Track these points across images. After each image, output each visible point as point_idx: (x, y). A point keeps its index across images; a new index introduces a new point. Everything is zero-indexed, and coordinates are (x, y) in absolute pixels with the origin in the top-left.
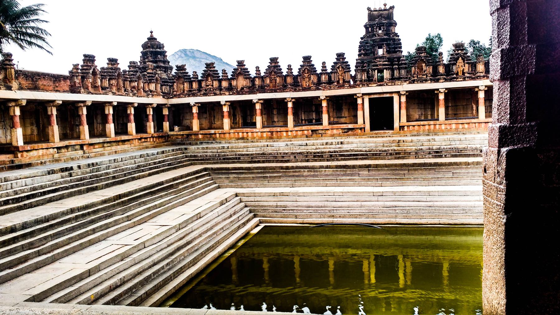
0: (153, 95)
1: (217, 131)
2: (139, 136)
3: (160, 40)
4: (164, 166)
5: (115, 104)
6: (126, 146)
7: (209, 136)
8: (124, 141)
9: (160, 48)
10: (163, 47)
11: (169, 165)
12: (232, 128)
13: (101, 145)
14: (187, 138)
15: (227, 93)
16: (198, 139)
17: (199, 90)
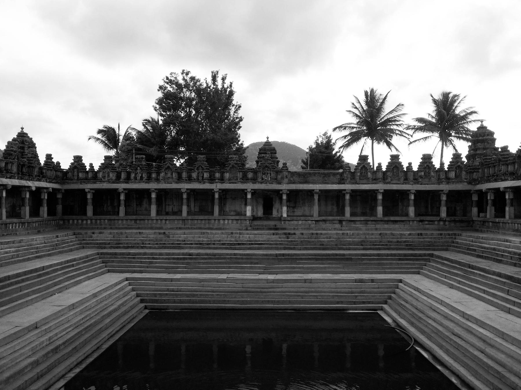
0: (448, 183)
1: (500, 219)
2: (418, 219)
3: (490, 128)
4: (397, 245)
5: (382, 191)
6: (397, 226)
7: (495, 224)
8: (396, 222)
9: (484, 136)
10: (491, 134)
11: (407, 245)
12: (516, 217)
13: (363, 222)
14: (483, 225)
15: (510, 179)
16: (488, 227)
17: (493, 176)
